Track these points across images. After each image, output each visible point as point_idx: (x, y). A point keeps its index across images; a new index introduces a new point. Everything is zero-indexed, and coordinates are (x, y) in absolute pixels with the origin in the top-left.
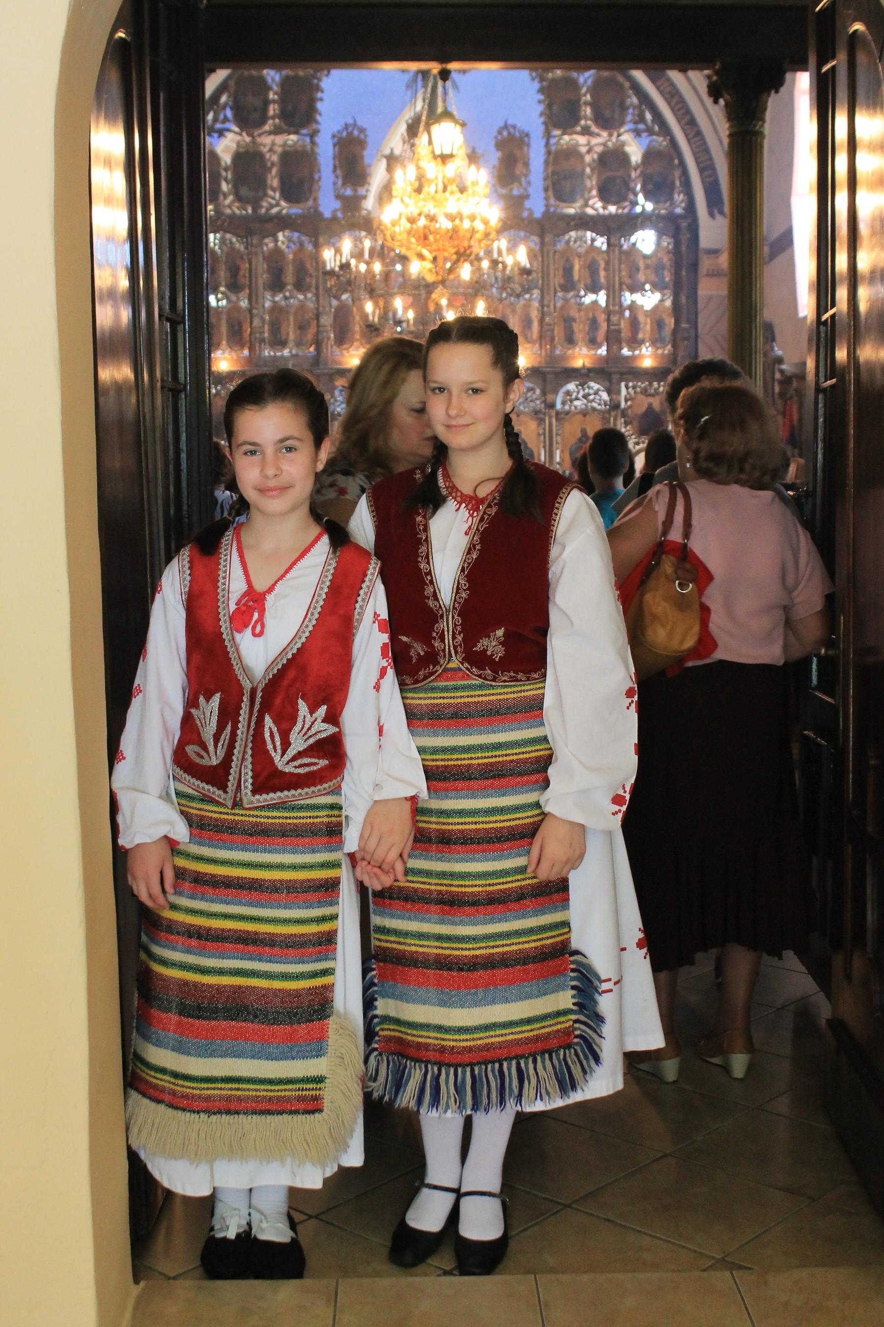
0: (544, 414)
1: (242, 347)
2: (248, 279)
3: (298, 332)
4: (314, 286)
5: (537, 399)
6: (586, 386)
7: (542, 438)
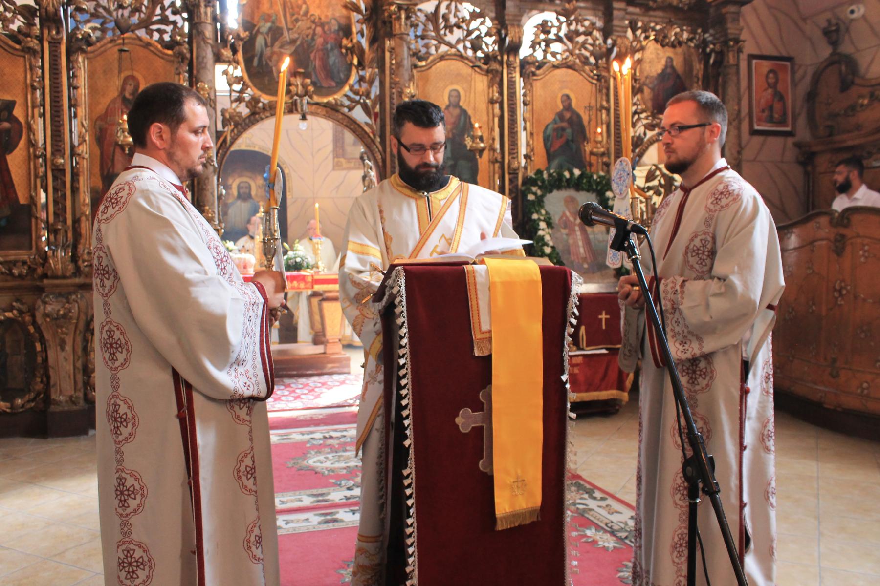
0: (501, 63)
6: (572, 18)
7: (497, 106)
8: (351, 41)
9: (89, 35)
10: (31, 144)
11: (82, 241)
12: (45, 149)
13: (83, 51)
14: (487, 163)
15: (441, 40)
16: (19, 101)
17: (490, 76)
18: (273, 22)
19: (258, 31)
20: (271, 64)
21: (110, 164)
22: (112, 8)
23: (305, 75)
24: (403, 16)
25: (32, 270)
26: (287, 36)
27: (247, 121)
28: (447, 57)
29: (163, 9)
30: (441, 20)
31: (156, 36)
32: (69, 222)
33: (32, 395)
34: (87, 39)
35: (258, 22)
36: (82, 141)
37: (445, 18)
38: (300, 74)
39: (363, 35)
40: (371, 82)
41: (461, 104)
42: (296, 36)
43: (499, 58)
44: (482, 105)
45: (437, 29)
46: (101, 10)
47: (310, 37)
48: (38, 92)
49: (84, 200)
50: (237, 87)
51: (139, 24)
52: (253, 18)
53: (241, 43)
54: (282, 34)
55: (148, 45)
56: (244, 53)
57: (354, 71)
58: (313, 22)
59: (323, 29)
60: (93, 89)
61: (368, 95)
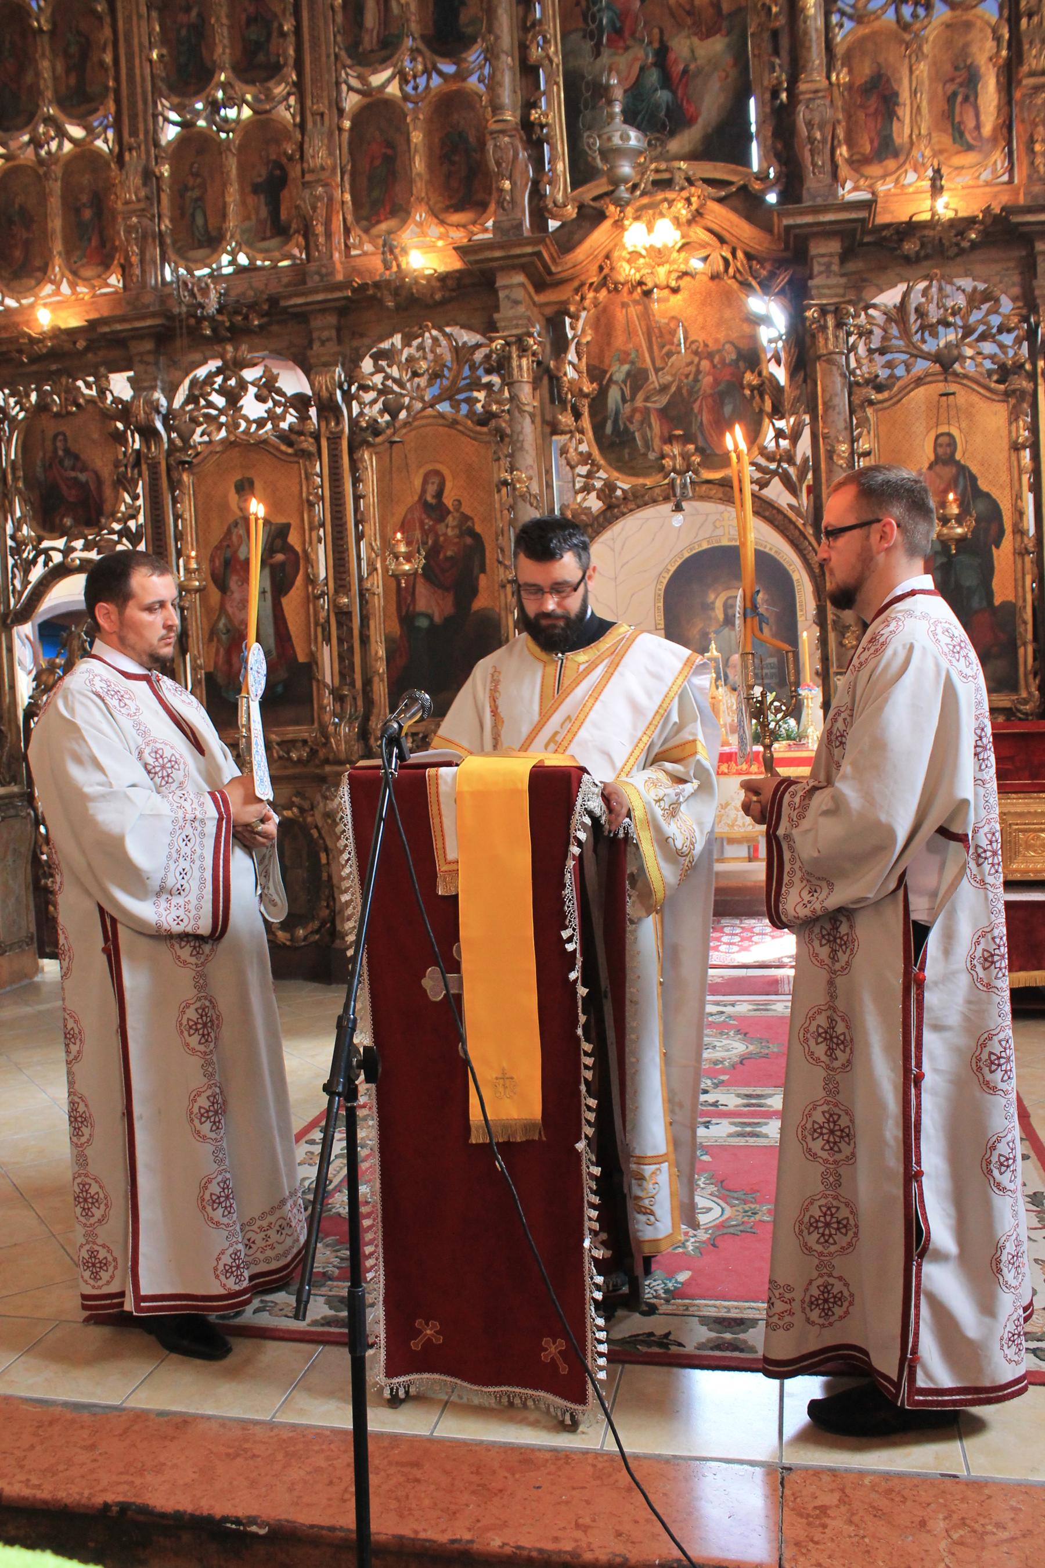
1: (106, 264)
2: (111, 72)
3: (251, 200)
4: (291, 62)
5: (1002, 329)
7: (1027, 454)
8: (760, 374)
9: (376, 421)
10: (310, 580)
11: (375, 711)
12: (327, 584)
13: (369, 445)
14: (1011, 556)
15: (915, 352)
16: (294, 522)
17: (1012, 401)
18: (632, 363)
19: (610, 379)
20: (632, 428)
21: (409, 598)
22: (405, 378)
23: (686, 439)
24: (830, 322)
25: (313, 753)
26: (654, 381)
27: (601, 519)
28: (929, 379)
29: (473, 368)
30: (913, 317)
31: (464, 408)
32: (359, 684)
33: (316, 924)
34: (374, 428)
35: (610, 366)
36: (372, 569)
37: (921, 313)
38: (678, 437)
39: (779, 363)
40: (795, 437)
41: (958, 456)
42: (669, 378)
43: (1028, 367)
44: (1000, 453)
45: (906, 333)
46: (389, 383)
47: (691, 377)
48: (318, 508)
49: (377, 653)
50: (583, 470)
51: (440, 395)
52: (602, 361)
53: (586, 402)
54: (647, 379)
55: (454, 423)
56: (592, 415)
57: (766, 421)
58: (696, 353)
59: (712, 362)
60: (386, 497)
61: (790, 459)
